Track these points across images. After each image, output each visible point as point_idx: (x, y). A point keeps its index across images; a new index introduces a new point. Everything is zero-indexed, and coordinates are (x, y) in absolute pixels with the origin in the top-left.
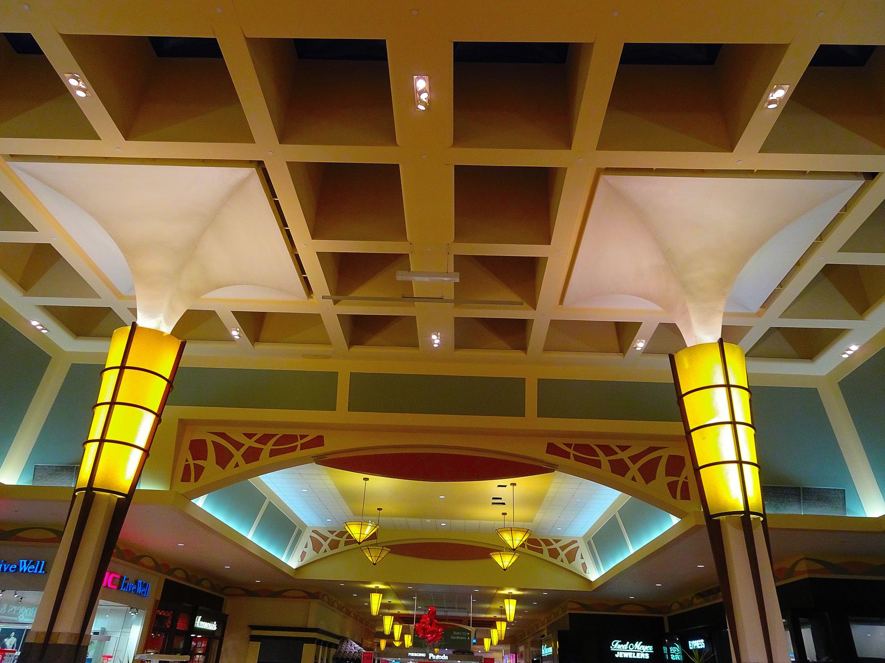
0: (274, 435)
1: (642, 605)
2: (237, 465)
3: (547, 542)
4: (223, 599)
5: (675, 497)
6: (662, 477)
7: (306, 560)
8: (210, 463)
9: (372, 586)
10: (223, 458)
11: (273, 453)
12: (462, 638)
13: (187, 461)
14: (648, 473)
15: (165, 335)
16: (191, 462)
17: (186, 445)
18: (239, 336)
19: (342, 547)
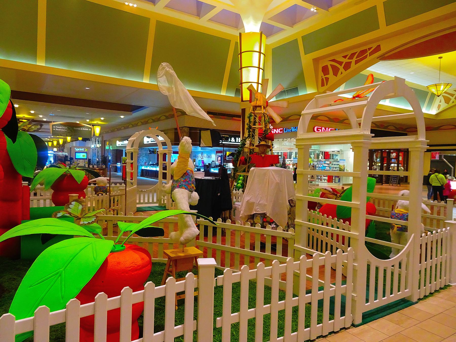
0: (356, 52)
2: (342, 73)
7: (441, 109)
8: (331, 75)
10: (336, 71)
11: (356, 62)
13: (322, 77)
15: (251, 33)
17: (320, 69)
18: (316, 10)
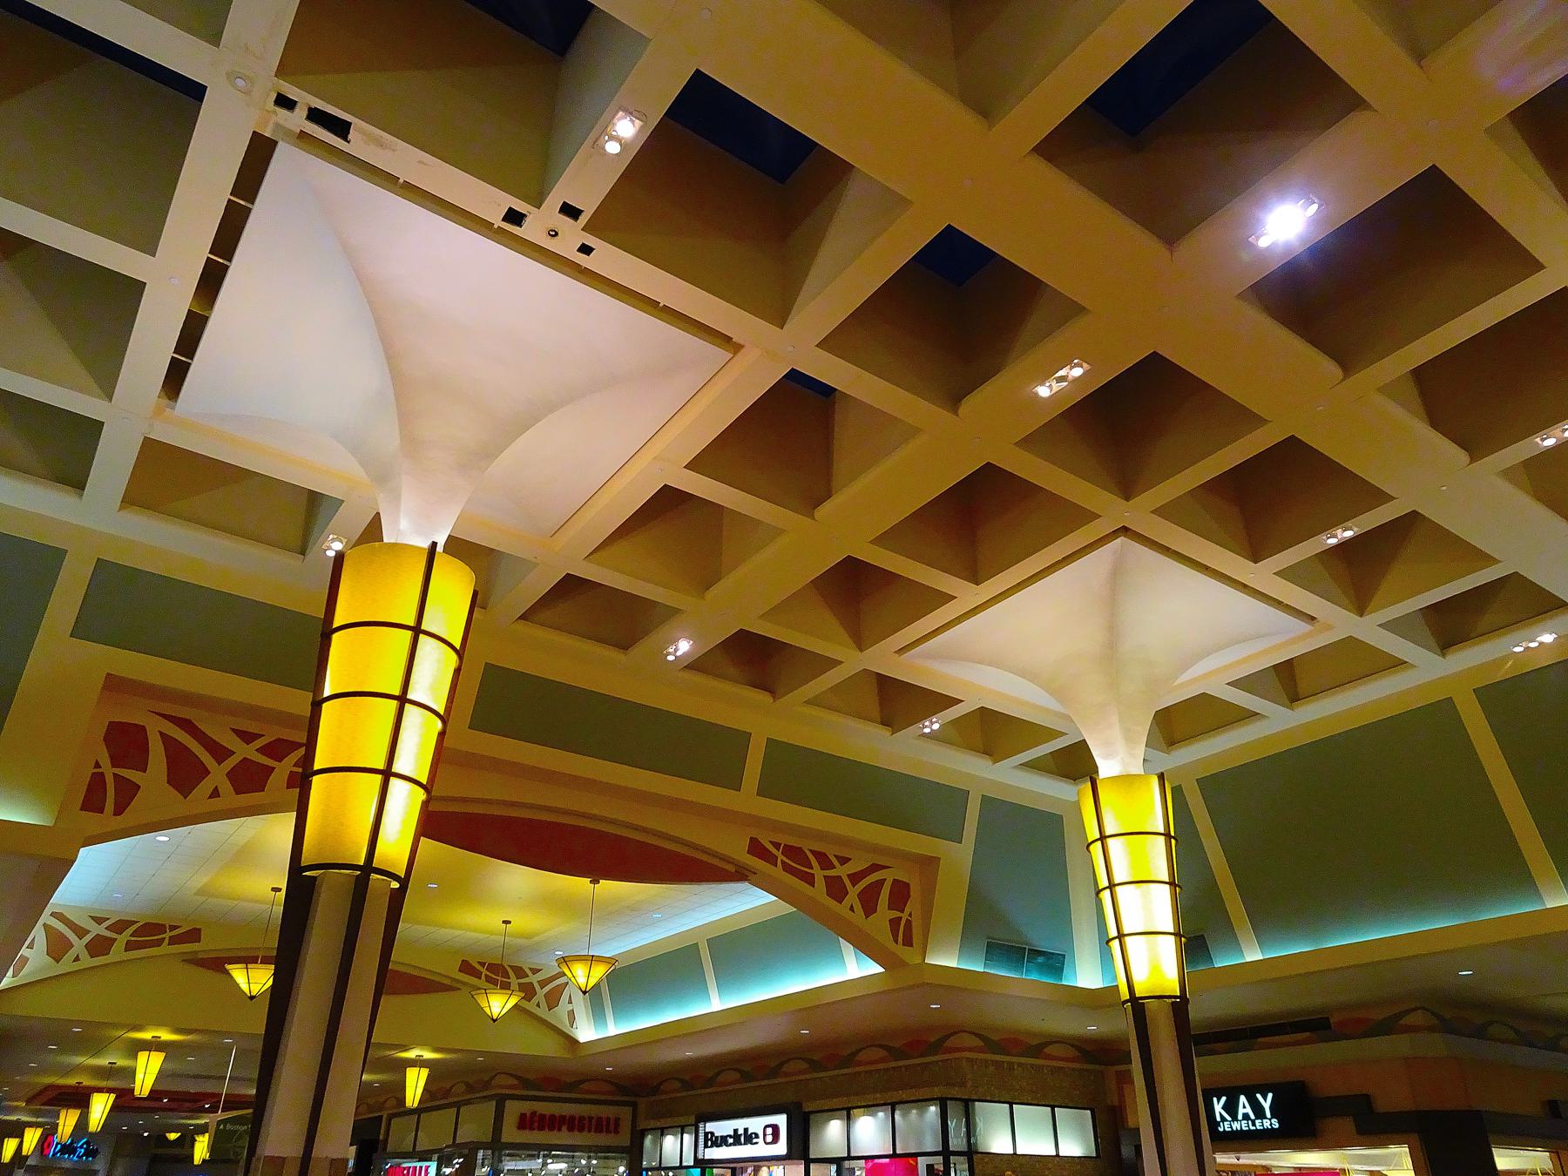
1: (611, 1082)
2: (215, 793)
3: (520, 972)
5: (896, 942)
6: (884, 913)
8: (153, 776)
9: (411, 1054)
10: (184, 774)
13: (97, 765)
14: (869, 902)
16: (108, 771)
19: (117, 953)
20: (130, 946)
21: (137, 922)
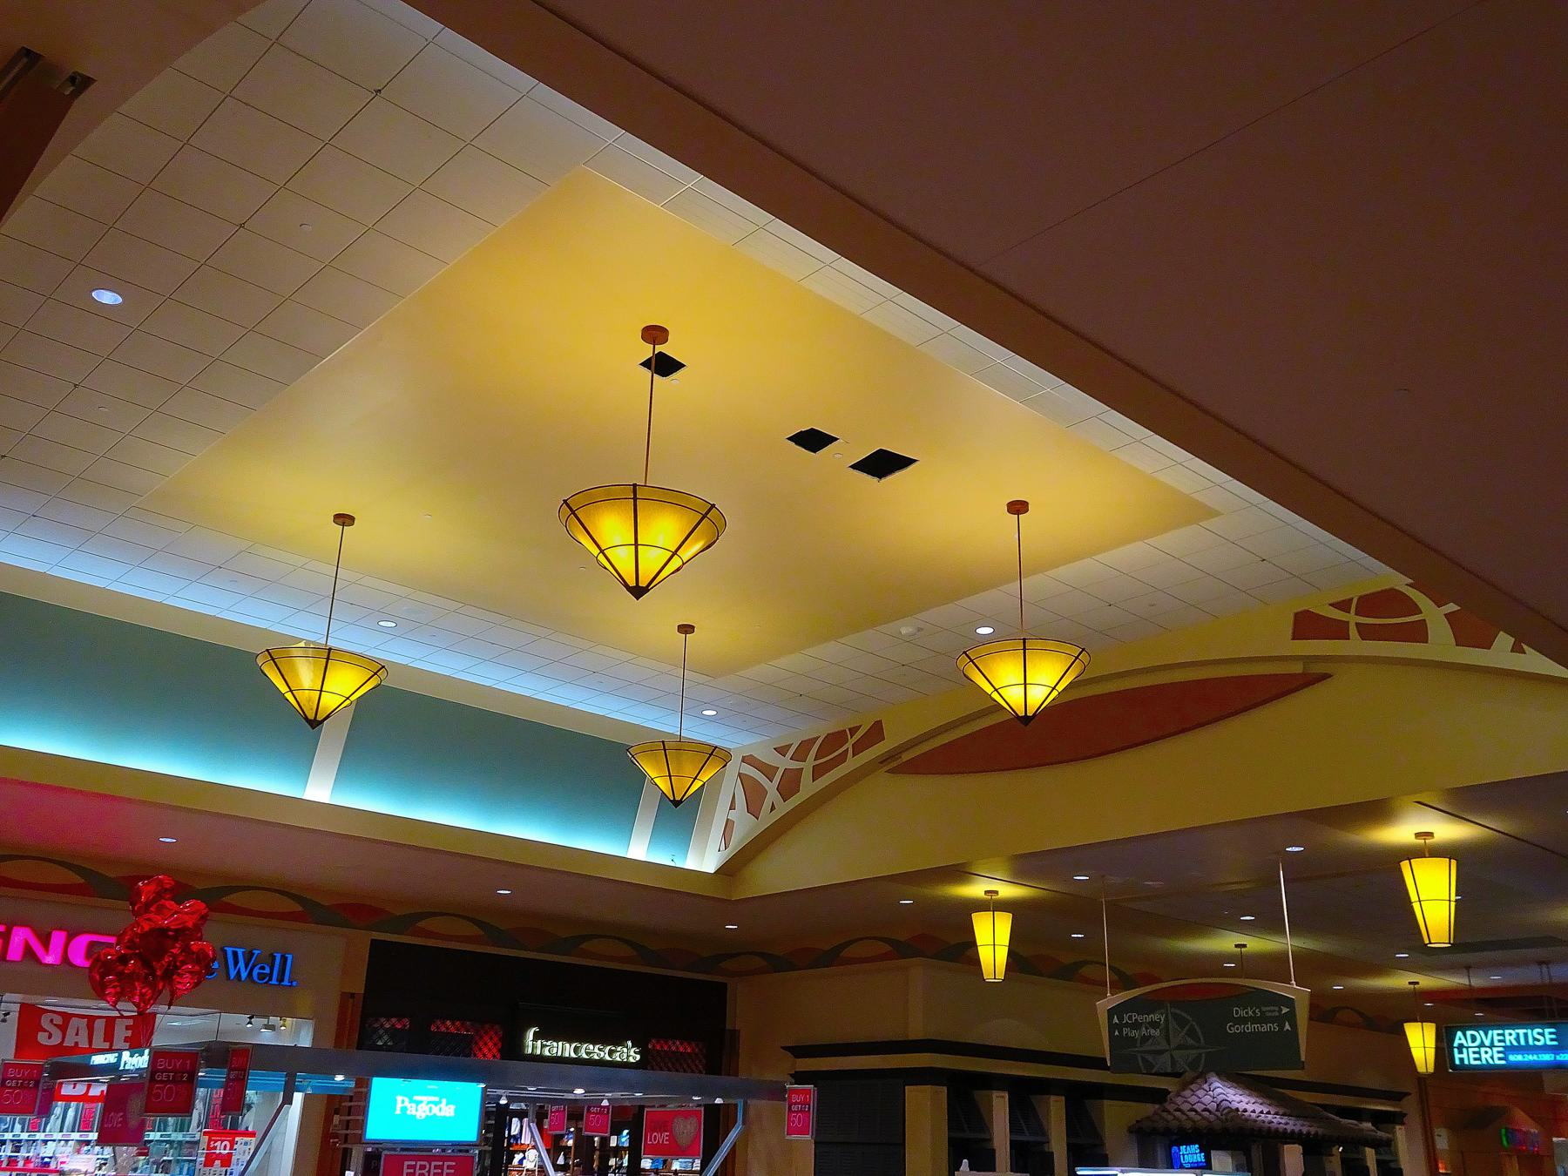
4: (725, 985)
12: (1265, 1028)
20: (818, 772)
21: (818, 738)
